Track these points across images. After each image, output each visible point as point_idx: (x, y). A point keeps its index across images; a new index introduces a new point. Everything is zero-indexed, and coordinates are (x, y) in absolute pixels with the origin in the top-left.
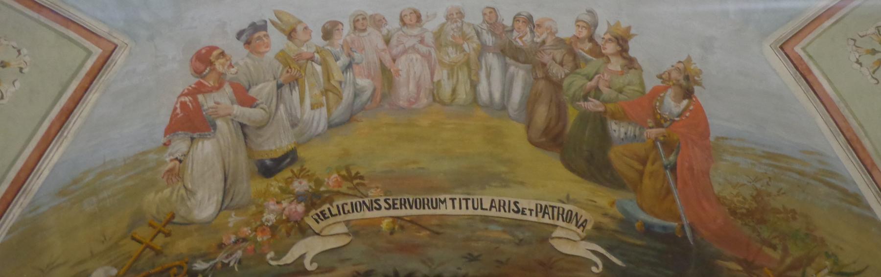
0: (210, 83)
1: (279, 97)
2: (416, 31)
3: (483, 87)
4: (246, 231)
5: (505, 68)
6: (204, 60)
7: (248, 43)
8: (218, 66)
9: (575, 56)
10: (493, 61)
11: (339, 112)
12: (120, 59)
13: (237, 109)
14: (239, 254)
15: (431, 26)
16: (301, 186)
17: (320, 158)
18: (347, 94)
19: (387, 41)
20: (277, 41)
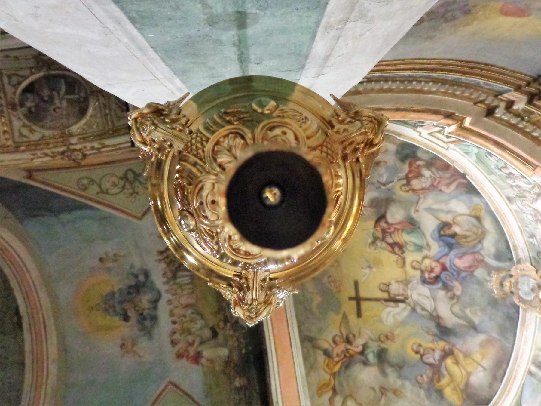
0: (186, 354)
1: (194, 334)
2: (173, 301)
3: (186, 282)
4: (235, 339)
5: (179, 277)
6: (179, 356)
7: (176, 344)
8: (181, 351)
9: (170, 262)
10: (178, 280)
11: (198, 317)
12: (175, 380)
13: (195, 345)
14: (242, 340)
15: (170, 297)
16: (222, 324)
17: (212, 320)
18: (193, 316)
19: (176, 307)
20: (177, 336)
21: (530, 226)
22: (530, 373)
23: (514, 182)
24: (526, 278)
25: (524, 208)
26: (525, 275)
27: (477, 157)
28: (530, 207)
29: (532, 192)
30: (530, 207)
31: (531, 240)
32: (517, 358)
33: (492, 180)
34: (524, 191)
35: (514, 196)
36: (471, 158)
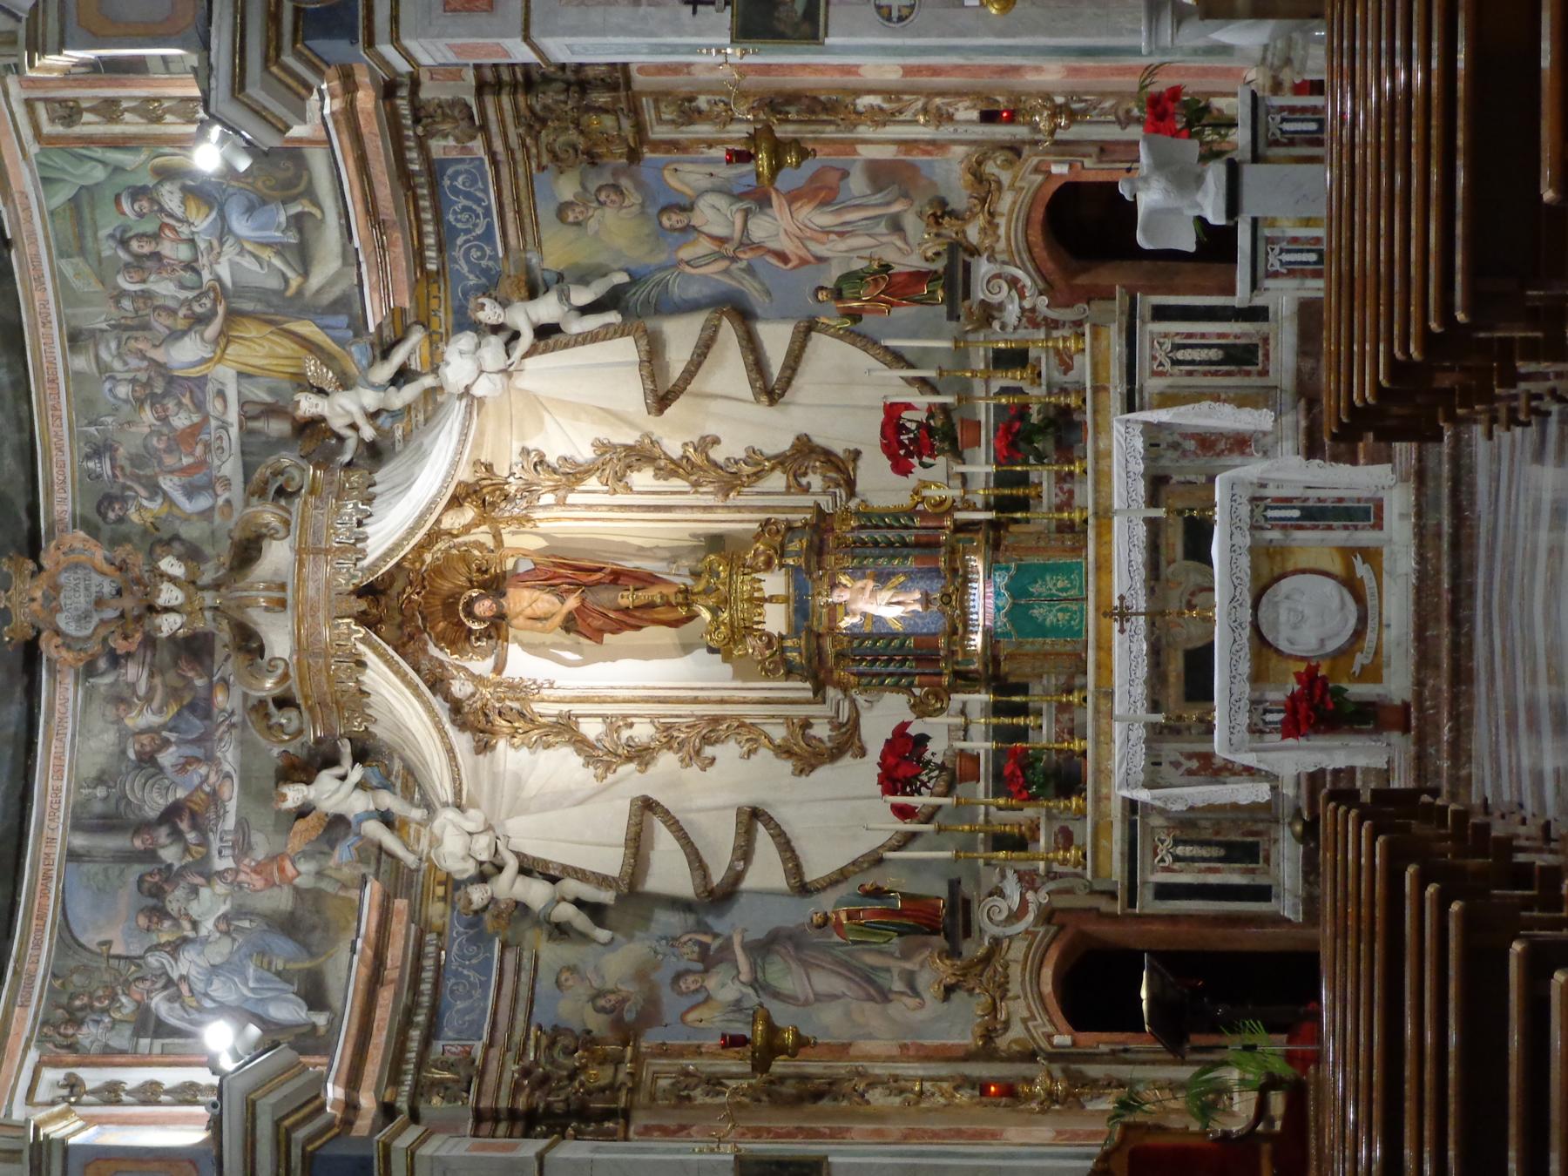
21: (109, 419)
22: (73, 856)
23: (144, 281)
24: (81, 573)
25: (117, 365)
26: (76, 566)
27: (75, 201)
28: (144, 357)
29: (181, 313)
30: (144, 357)
31: (91, 464)
32: (42, 823)
33: (61, 272)
34: (156, 308)
35: (104, 326)
36: (48, 197)
